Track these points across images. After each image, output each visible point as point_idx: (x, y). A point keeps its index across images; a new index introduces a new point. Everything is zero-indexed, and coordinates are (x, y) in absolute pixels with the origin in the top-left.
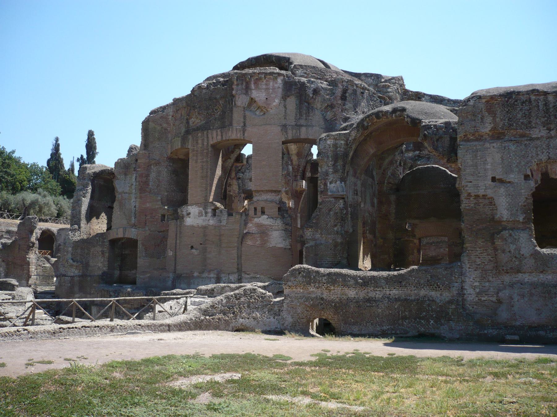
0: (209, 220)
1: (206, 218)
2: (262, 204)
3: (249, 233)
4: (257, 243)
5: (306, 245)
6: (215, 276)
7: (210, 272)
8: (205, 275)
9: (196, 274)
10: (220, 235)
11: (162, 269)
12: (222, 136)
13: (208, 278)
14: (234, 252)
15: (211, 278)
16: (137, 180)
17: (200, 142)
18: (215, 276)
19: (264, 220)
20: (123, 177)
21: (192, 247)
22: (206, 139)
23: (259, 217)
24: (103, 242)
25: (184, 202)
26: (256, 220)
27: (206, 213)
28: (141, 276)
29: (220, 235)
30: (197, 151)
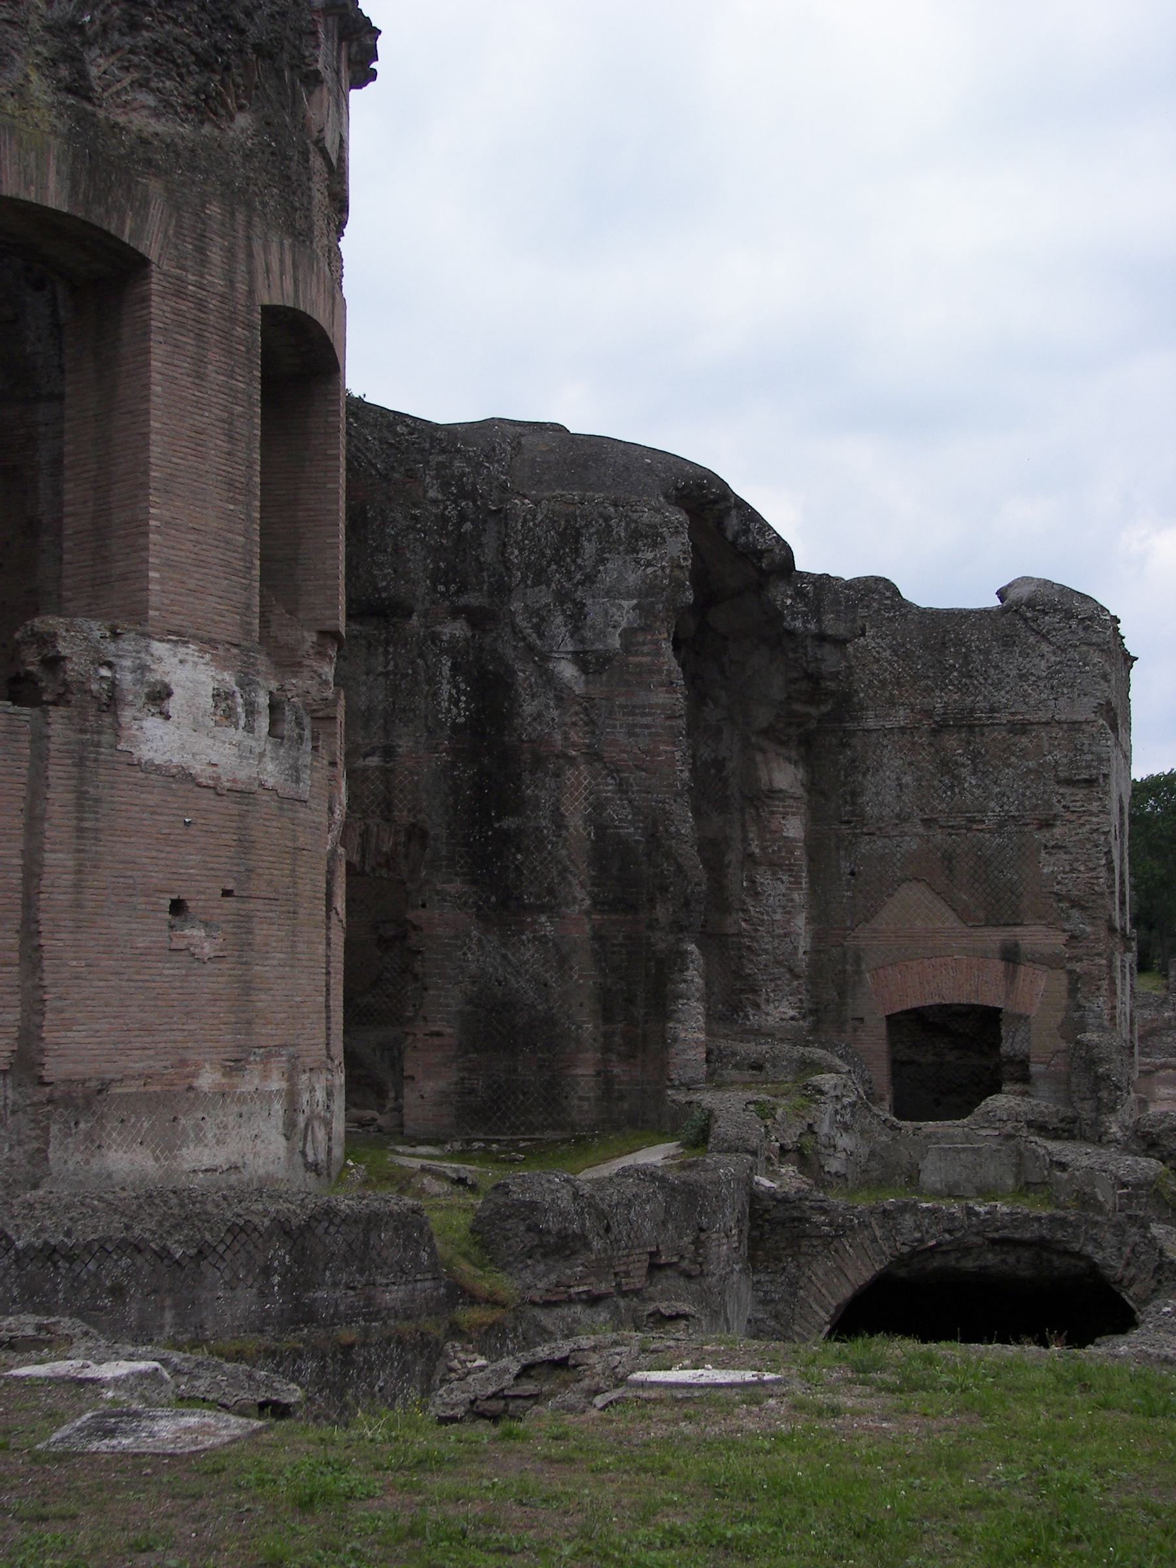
9: (208, 1079)
17: (216, 255)
21: (178, 907)
22: (241, 256)
27: (251, 710)
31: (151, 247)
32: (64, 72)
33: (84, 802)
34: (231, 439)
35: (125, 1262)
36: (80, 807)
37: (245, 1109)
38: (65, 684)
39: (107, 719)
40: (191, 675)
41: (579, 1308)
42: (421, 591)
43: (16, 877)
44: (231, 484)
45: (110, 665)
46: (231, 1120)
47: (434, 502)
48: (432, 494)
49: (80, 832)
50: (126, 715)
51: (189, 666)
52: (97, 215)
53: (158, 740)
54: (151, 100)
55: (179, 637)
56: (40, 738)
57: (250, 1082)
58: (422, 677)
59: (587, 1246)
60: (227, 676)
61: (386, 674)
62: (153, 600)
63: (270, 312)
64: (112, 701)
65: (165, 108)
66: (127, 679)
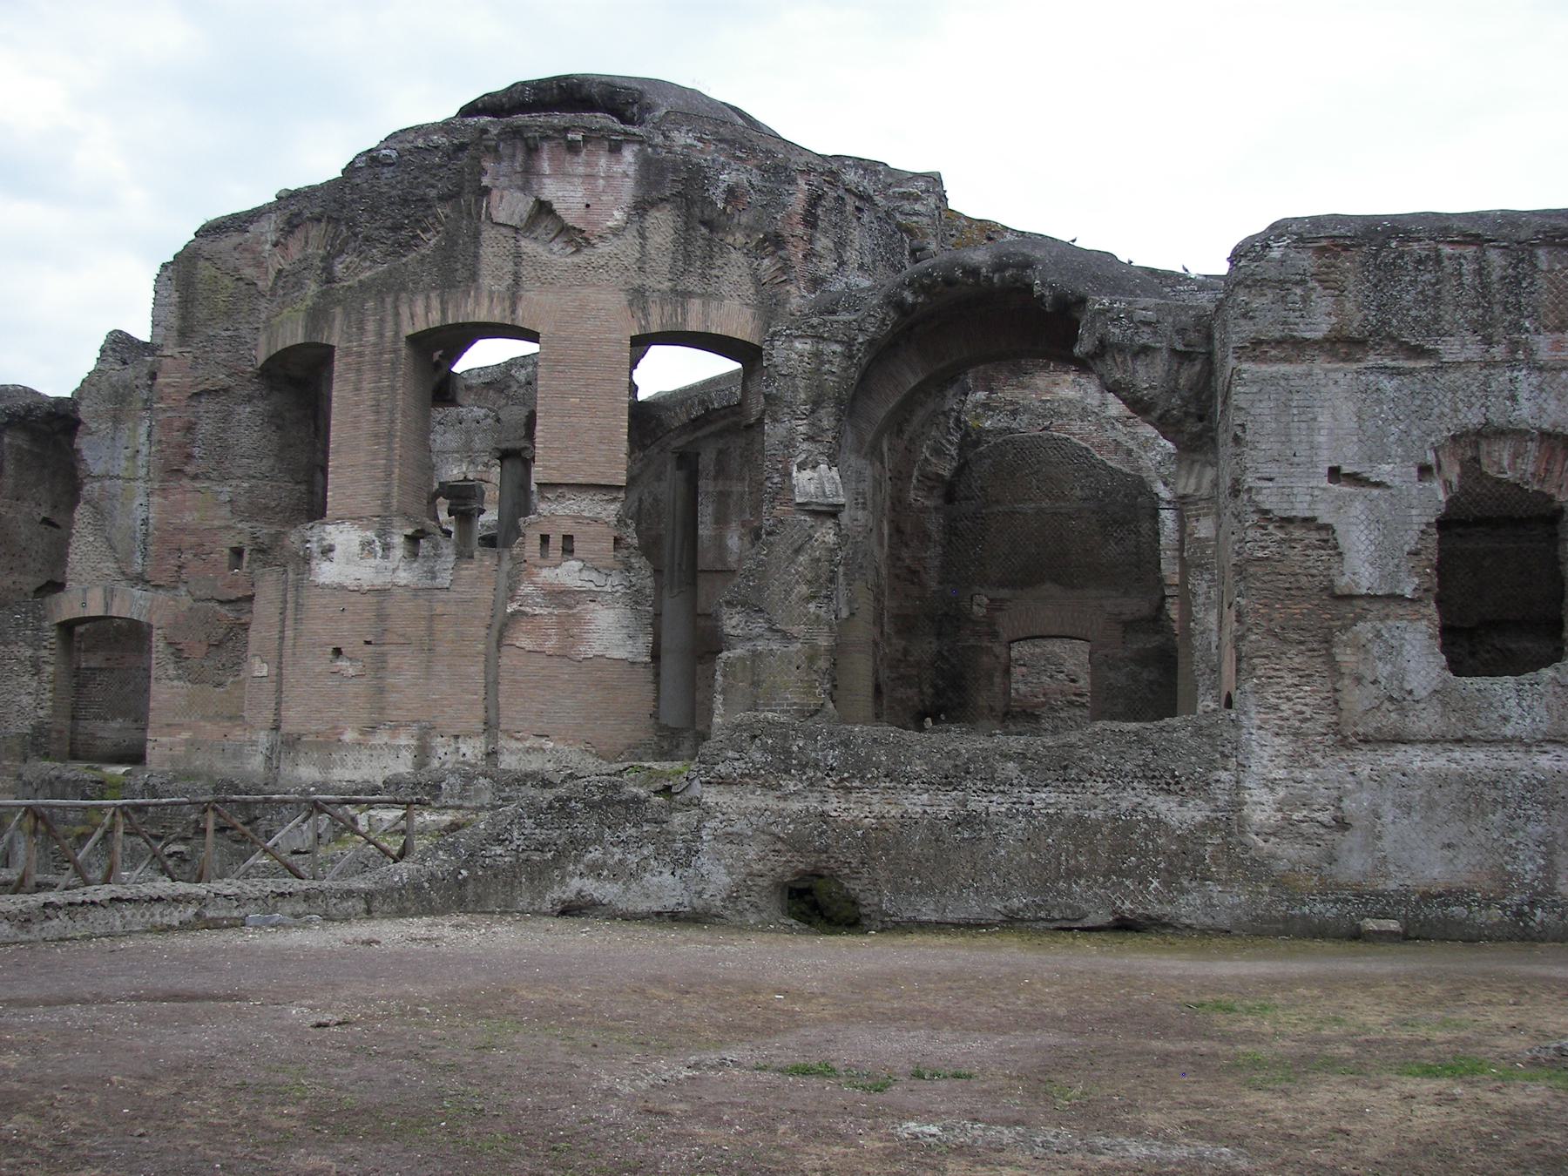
0: (394, 570)
2: (567, 527)
3: (525, 614)
4: (548, 644)
5: (725, 654)
6: (413, 742)
7: (395, 728)
8: (381, 738)
9: (349, 736)
10: (432, 618)
11: (230, 718)
12: (444, 312)
14: (476, 670)
16: (155, 438)
17: (371, 326)
18: (413, 742)
19: (569, 574)
20: (105, 427)
21: (338, 652)
22: (390, 319)
23: (556, 566)
25: (314, 509)
26: (545, 572)
27: (387, 548)
28: (164, 740)
29: (432, 618)
30: (360, 355)
46: (364, 758)
64: (307, 560)
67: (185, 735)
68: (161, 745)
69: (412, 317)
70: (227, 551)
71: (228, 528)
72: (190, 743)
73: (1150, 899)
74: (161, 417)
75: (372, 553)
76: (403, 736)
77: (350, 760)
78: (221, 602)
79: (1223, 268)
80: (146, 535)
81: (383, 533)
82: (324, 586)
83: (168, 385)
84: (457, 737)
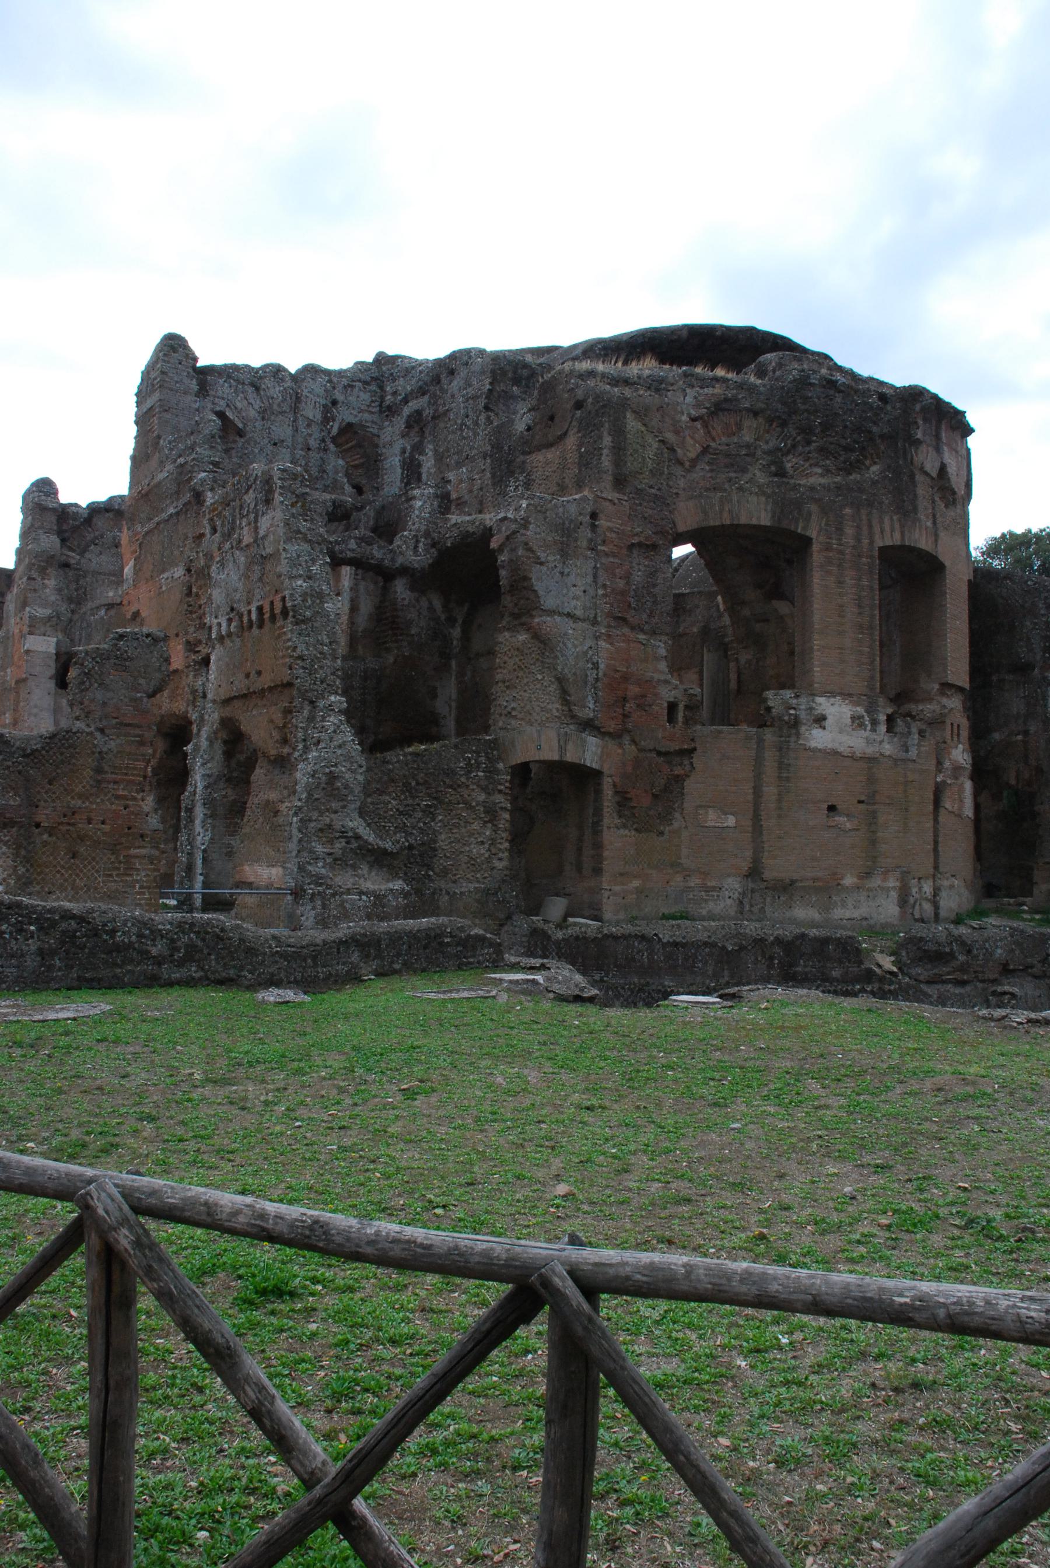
0: (881, 742)
1: (874, 736)
6: (898, 884)
7: (886, 873)
9: (849, 881)
13: (882, 888)
14: (930, 824)
15: (888, 889)
16: (600, 580)
17: (849, 531)
18: (898, 884)
20: (553, 558)
21: (832, 808)
22: (865, 528)
24: (491, 771)
27: (874, 723)
28: (617, 888)
31: (813, 533)
32: (773, 468)
33: (781, 766)
34: (860, 606)
35: (707, 950)
36: (780, 768)
37: (871, 894)
38: (773, 718)
39: (794, 731)
40: (837, 711)
41: (950, 985)
42: (1038, 658)
43: (750, 797)
44: (861, 626)
45: (794, 709)
46: (862, 898)
47: (1043, 615)
48: (1042, 612)
49: (780, 778)
50: (803, 729)
51: (836, 706)
52: (785, 524)
53: (818, 738)
54: (820, 471)
55: (832, 694)
56: (760, 741)
57: (876, 882)
58: (1040, 697)
59: (955, 958)
60: (859, 709)
61: (1024, 697)
62: (816, 680)
63: (883, 550)
64: (796, 723)
65: (827, 471)
66: (803, 715)
67: (636, 883)
68: (615, 894)
69: (882, 532)
70: (666, 705)
71: (666, 682)
72: (639, 891)
73: (512, 986)
74: (604, 560)
75: (862, 726)
76: (891, 879)
77: (850, 902)
78: (659, 753)
79: (84, 506)
80: (597, 680)
81: (871, 709)
82: (815, 750)
83: (610, 529)
84: (920, 879)
